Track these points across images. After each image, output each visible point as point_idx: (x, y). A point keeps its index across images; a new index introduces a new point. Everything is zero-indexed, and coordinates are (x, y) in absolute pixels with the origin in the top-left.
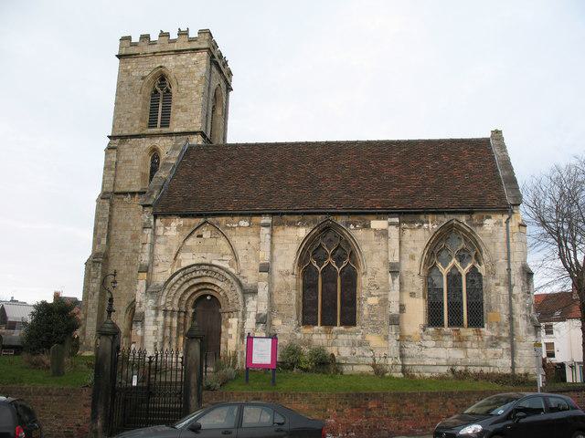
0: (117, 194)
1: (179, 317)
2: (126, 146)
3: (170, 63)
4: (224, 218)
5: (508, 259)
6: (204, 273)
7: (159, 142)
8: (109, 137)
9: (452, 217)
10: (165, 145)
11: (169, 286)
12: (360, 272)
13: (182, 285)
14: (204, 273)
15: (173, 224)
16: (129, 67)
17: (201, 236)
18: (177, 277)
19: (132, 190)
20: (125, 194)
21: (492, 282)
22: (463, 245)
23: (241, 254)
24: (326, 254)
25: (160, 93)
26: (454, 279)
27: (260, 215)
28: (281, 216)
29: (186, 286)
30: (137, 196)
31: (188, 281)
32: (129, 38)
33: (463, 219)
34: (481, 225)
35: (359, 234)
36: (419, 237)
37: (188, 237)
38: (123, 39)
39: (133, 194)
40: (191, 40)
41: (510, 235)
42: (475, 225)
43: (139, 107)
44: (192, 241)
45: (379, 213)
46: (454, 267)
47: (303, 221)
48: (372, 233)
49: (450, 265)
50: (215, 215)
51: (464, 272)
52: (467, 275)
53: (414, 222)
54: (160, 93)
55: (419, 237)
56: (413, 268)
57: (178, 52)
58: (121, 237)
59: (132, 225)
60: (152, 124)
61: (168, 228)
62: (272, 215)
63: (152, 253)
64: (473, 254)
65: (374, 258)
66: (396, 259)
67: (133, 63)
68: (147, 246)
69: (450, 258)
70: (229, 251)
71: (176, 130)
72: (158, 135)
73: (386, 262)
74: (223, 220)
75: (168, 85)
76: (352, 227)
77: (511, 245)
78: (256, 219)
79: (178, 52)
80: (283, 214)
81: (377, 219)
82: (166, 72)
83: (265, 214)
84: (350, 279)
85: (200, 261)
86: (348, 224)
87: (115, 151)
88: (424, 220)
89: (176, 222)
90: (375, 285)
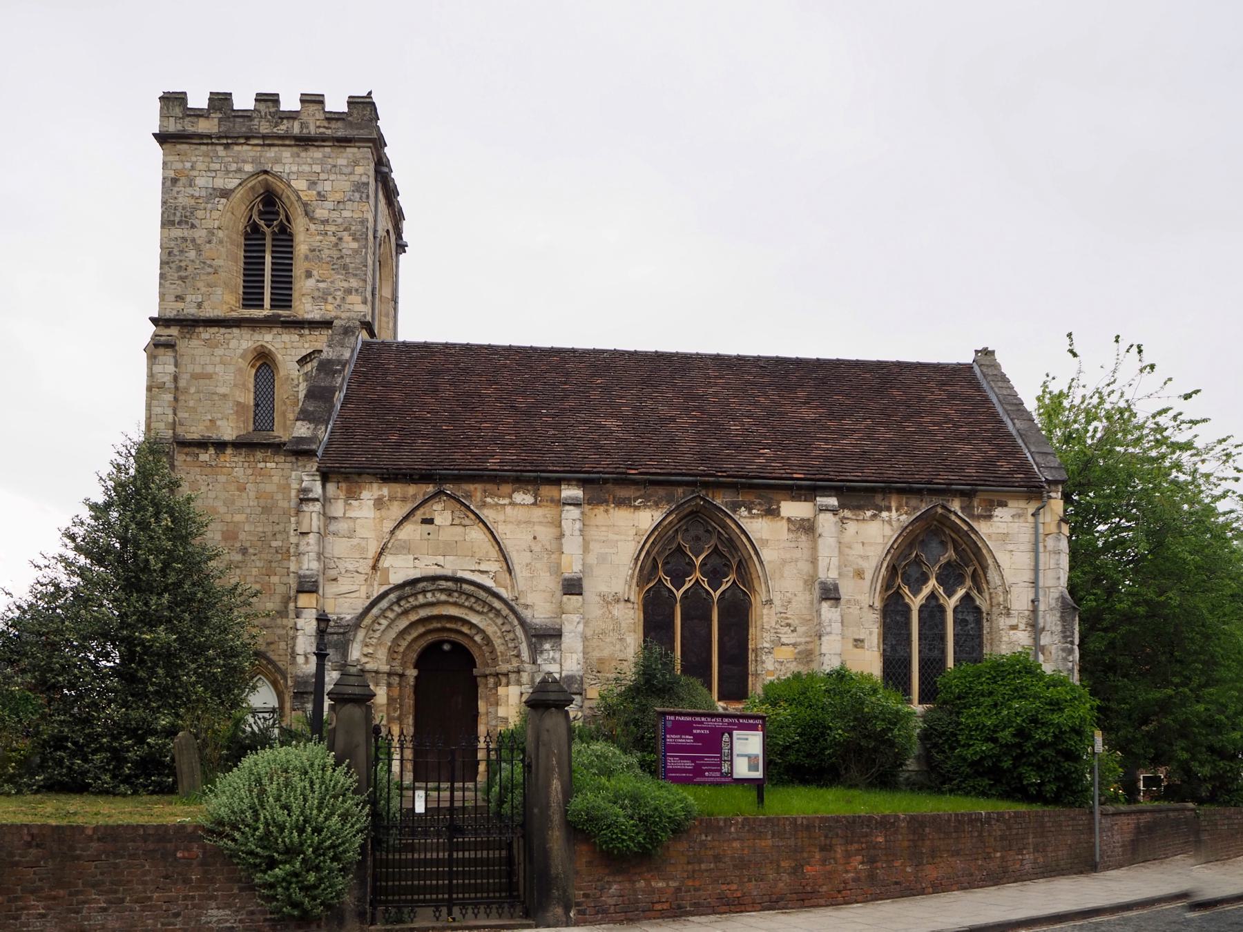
1: (389, 685)
2: (195, 343)
3: (294, 170)
4: (479, 487)
5: (1035, 583)
6: (443, 597)
7: (272, 340)
8: (153, 320)
9: (936, 500)
11: (367, 621)
12: (757, 600)
13: (393, 621)
14: (443, 597)
17: (429, 521)
18: (384, 604)
21: (1003, 622)
22: (950, 554)
23: (518, 560)
24: (692, 564)
26: (933, 610)
27: (558, 482)
28: (605, 485)
29: (403, 623)
31: (405, 613)
33: (956, 505)
34: (990, 517)
35: (757, 527)
36: (873, 535)
37: (401, 523)
41: (1041, 537)
42: (979, 517)
44: (411, 531)
45: (800, 488)
46: (933, 596)
47: (647, 498)
48: (784, 524)
49: (926, 591)
50: (459, 479)
51: (951, 603)
52: (955, 610)
53: (860, 508)
55: (873, 535)
56: (863, 598)
60: (252, 297)
62: (583, 483)
63: (320, 556)
64: (970, 570)
65: (786, 573)
66: (833, 574)
68: (312, 538)
69: (924, 579)
70: (494, 553)
71: (309, 316)
73: (811, 580)
74: (477, 489)
76: (743, 511)
77: (1042, 557)
78: (546, 491)
80: (606, 481)
81: (793, 499)
83: (568, 481)
84: (738, 615)
85: (433, 571)
86: (735, 507)
87: (170, 353)
88: (883, 504)
89: (371, 492)
90: (789, 625)
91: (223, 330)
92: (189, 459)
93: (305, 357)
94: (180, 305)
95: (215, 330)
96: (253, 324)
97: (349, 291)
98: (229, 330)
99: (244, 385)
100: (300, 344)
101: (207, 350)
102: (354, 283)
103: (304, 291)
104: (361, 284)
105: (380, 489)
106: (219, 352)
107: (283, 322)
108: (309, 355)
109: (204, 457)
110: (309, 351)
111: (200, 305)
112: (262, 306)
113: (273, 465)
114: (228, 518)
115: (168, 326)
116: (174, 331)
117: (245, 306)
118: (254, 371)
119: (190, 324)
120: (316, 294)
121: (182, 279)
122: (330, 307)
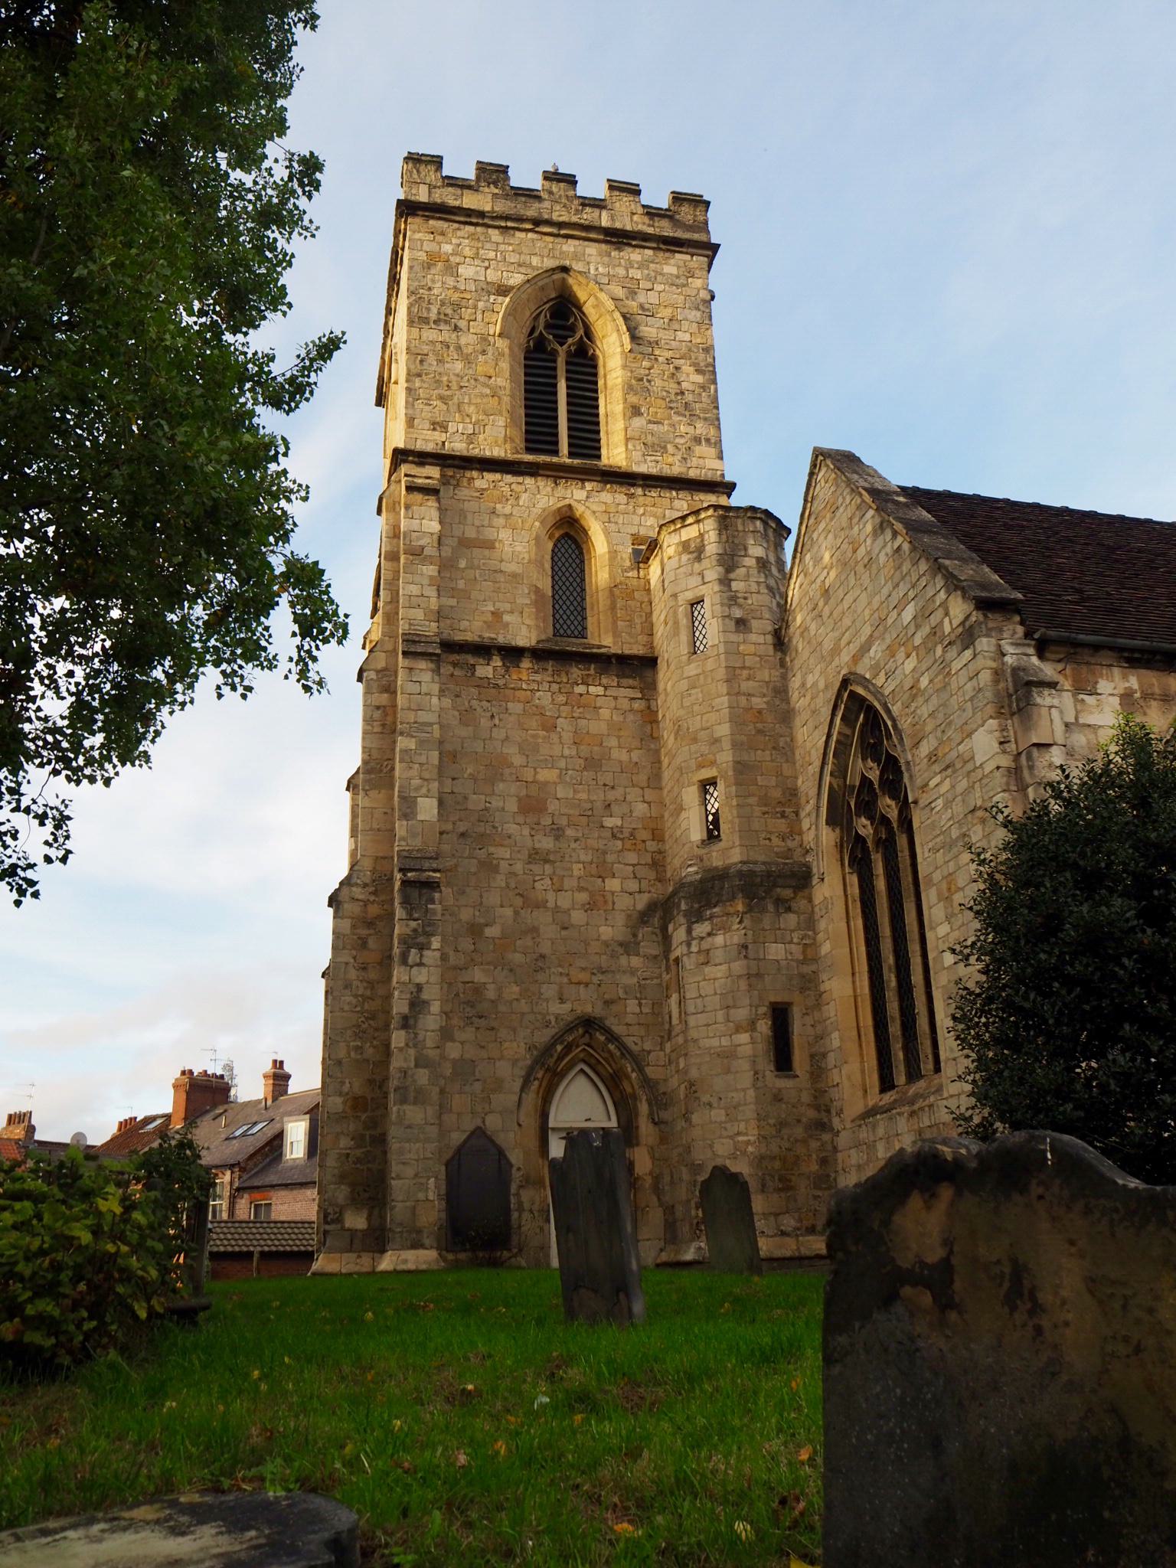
0: (450, 647)
2: (464, 493)
15: (1104, 686)
16: (447, 248)
20: (483, 650)
30: (526, 663)
32: (437, 162)
38: (414, 159)
39: (512, 654)
40: (652, 213)
43: (501, 373)
57: (618, 238)
58: (476, 802)
59: (518, 760)
61: (1090, 700)
67: (455, 240)
72: (582, 475)
75: (581, 332)
79: (618, 238)
87: (432, 502)
91: (509, 478)
96: (558, 473)
97: (697, 440)
98: (520, 479)
102: (701, 429)
104: (712, 431)
105: (1125, 677)
115: (422, 464)
116: (434, 472)
117: (529, 450)
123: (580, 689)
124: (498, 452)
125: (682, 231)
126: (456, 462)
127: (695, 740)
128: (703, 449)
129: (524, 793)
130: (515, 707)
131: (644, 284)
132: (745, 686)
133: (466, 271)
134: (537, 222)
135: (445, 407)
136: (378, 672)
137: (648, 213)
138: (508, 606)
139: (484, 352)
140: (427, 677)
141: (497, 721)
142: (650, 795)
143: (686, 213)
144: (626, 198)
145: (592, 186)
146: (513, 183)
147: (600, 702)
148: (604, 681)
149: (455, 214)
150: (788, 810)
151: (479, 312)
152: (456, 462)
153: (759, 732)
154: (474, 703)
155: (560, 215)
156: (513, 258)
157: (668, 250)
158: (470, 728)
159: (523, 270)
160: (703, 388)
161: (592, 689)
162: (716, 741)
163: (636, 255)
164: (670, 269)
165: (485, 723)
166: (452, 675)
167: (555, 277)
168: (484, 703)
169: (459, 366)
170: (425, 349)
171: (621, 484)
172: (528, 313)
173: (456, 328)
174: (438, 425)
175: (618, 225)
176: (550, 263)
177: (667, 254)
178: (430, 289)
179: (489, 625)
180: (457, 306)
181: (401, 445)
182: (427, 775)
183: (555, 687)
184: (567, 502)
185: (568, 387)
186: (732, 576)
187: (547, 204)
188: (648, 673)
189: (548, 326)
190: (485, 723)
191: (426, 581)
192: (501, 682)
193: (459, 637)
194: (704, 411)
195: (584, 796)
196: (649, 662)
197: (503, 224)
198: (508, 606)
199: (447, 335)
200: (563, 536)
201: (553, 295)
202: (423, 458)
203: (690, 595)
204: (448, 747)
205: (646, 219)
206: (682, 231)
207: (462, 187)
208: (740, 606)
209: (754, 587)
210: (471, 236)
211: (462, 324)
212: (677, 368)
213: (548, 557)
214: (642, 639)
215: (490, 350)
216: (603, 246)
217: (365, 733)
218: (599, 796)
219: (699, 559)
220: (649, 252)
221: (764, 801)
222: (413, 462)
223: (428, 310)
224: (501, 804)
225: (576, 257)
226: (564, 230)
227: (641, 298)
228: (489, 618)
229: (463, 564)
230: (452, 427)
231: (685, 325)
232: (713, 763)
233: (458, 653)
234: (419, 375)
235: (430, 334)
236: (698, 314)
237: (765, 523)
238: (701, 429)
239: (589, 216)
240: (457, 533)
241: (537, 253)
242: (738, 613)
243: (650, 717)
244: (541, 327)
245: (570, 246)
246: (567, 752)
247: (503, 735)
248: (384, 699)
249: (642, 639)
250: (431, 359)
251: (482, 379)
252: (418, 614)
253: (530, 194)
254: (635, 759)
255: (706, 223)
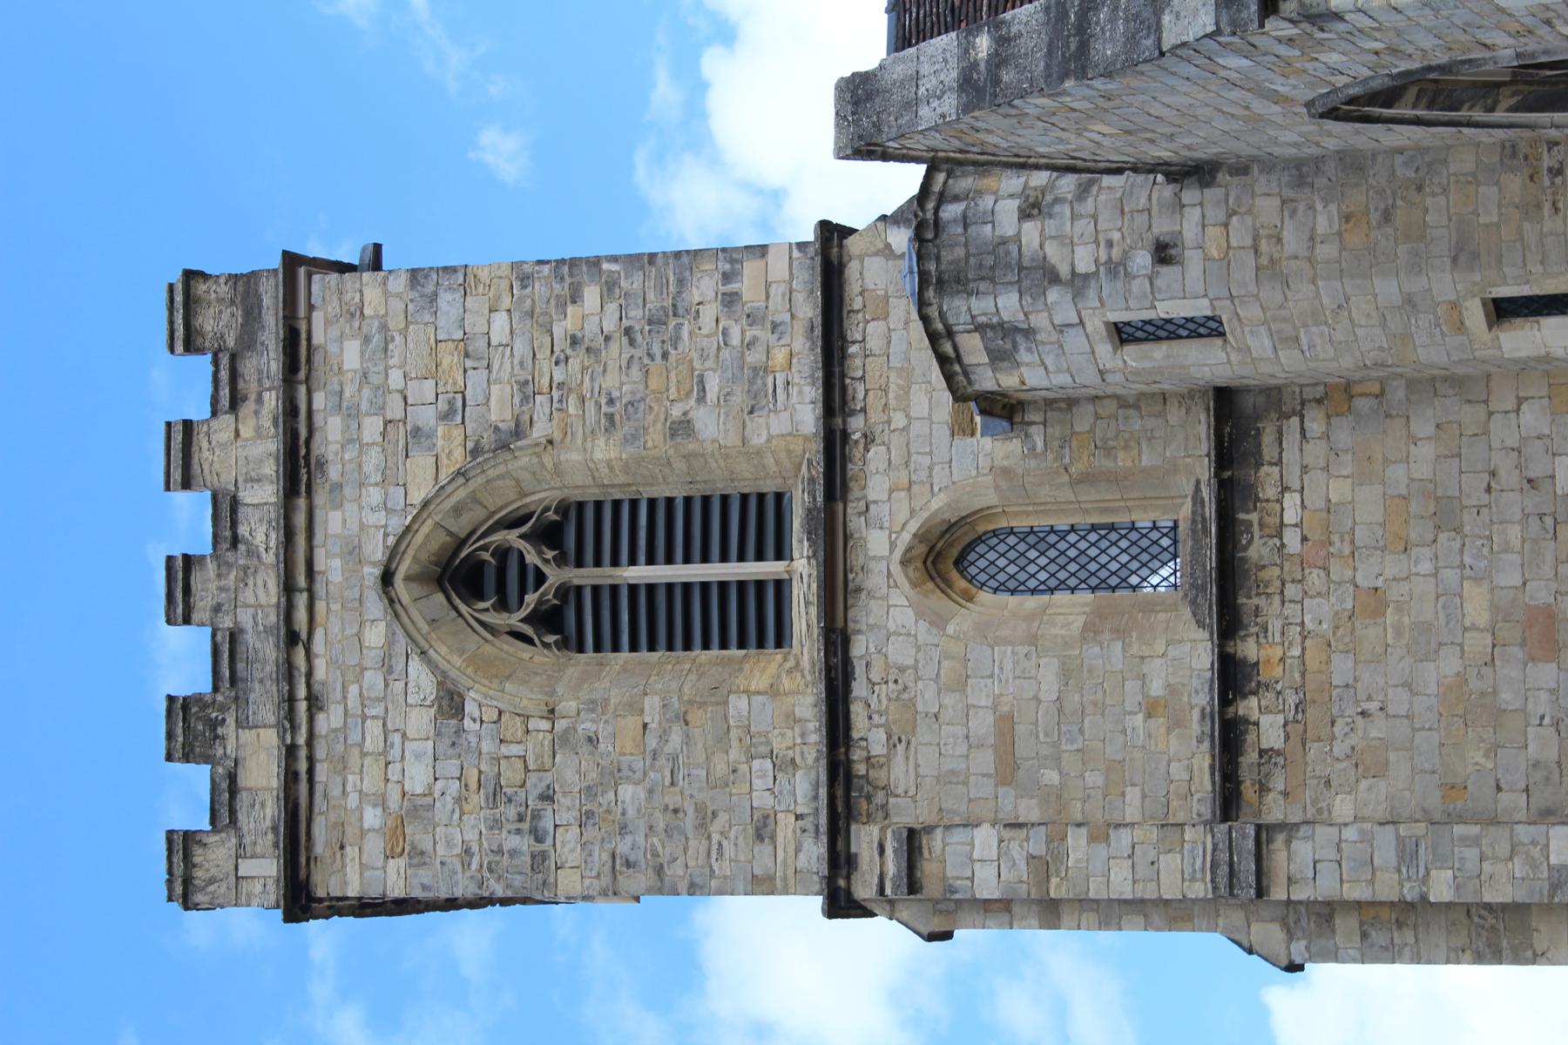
0: (1228, 802)
2: (899, 774)
10: (923, 462)
19: (1200, 695)
25: (556, 574)
30: (1248, 649)
32: (182, 845)
38: (185, 890)
39: (1232, 677)
40: (230, 396)
43: (631, 698)
54: (556, 574)
57: (298, 468)
59: (1450, 664)
60: (753, 619)
71: (808, 417)
75: (512, 537)
79: (298, 468)
82: (427, 542)
87: (935, 843)
91: (859, 688)
92: (1278, 783)
93: (943, 360)
94: (786, 827)
95: (858, 712)
96: (836, 591)
97: (730, 300)
98: (859, 670)
99: (1030, 617)
100: (896, 441)
101: (923, 733)
102: (705, 287)
103: (732, 440)
106: (927, 698)
107: (830, 496)
108: (933, 338)
109: (1269, 730)
110: (917, 326)
111: (784, 765)
112: (781, 586)
113: (1291, 501)
114: (1478, 643)
116: (864, 838)
118: (985, 596)
119: (844, 790)
120: (739, 398)
121: (705, 817)
122: (780, 356)
123: (1292, 539)
124: (808, 704)
125: (261, 331)
126: (840, 792)
127: (1407, 337)
128: (748, 285)
129: (1517, 652)
130: (1342, 668)
131: (395, 409)
132: (1293, 240)
133: (418, 777)
134: (292, 638)
135: (723, 818)
136: (1291, 937)
137: (234, 405)
138: (1132, 686)
139: (592, 741)
140: (1303, 850)
141: (1373, 706)
142: (1503, 399)
143: (217, 321)
144: (204, 454)
145: (188, 522)
146: (204, 685)
147: (1315, 500)
148: (1270, 492)
149: (296, 805)
150: (1547, 161)
151: (505, 750)
152: (840, 792)
153: (1387, 217)
154: (1340, 749)
155: (265, 591)
156: (374, 679)
157: (309, 361)
158: (1392, 756)
159: (399, 665)
160: (610, 286)
161: (1290, 517)
162: (1409, 301)
163: (331, 433)
164: (351, 355)
165: (1377, 729)
166: (1286, 794)
167: (406, 599)
168: (1339, 729)
169: (627, 792)
170: (600, 857)
171: (845, 459)
172: (488, 648)
173: (548, 797)
174: (763, 830)
175: (270, 468)
176: (375, 606)
177: (318, 358)
178: (467, 851)
179: (1176, 723)
180: (497, 794)
181: (818, 901)
182: (1504, 848)
183: (1291, 590)
184: (896, 569)
185: (633, 561)
186: (1064, 271)
187: (245, 618)
188: (1248, 403)
189: (503, 605)
190: (1377, 729)
191: (1101, 850)
192: (1292, 699)
193: (1205, 784)
194: (662, 285)
195: (1514, 532)
196: (1224, 400)
197: (302, 706)
198: (1132, 686)
199: (566, 811)
200: (962, 572)
201: (440, 597)
202: (840, 861)
203: (1104, 350)
204: (1434, 801)
205: (247, 408)
206: (261, 331)
207: (233, 791)
208: (1126, 255)
209: (1085, 226)
210: (342, 766)
211: (536, 785)
212: (574, 341)
213: (1013, 601)
214: (1175, 415)
215: (586, 726)
216: (320, 498)
217: (1417, 959)
218: (1513, 503)
219: (1029, 333)
220: (319, 400)
221: (1530, 209)
222: (848, 878)
223: (513, 853)
224: (1544, 696)
225: (353, 552)
226: (298, 575)
227: (426, 417)
228: (1159, 723)
229: (1051, 777)
230: (763, 800)
231: (475, 323)
232: (1454, 305)
233: (1239, 783)
234: (659, 870)
235: (567, 846)
236: (445, 298)
237: (942, 199)
238: (705, 287)
239: (260, 531)
240: (986, 788)
241: (355, 635)
242: (1142, 260)
243: (1338, 396)
244: (514, 620)
245: (330, 565)
246: (1426, 567)
247: (1403, 695)
248: (1346, 925)
249: (1175, 415)
250: (624, 847)
251: (652, 742)
252: (1170, 863)
253: (228, 652)
254: (1430, 429)
255: (234, 278)
